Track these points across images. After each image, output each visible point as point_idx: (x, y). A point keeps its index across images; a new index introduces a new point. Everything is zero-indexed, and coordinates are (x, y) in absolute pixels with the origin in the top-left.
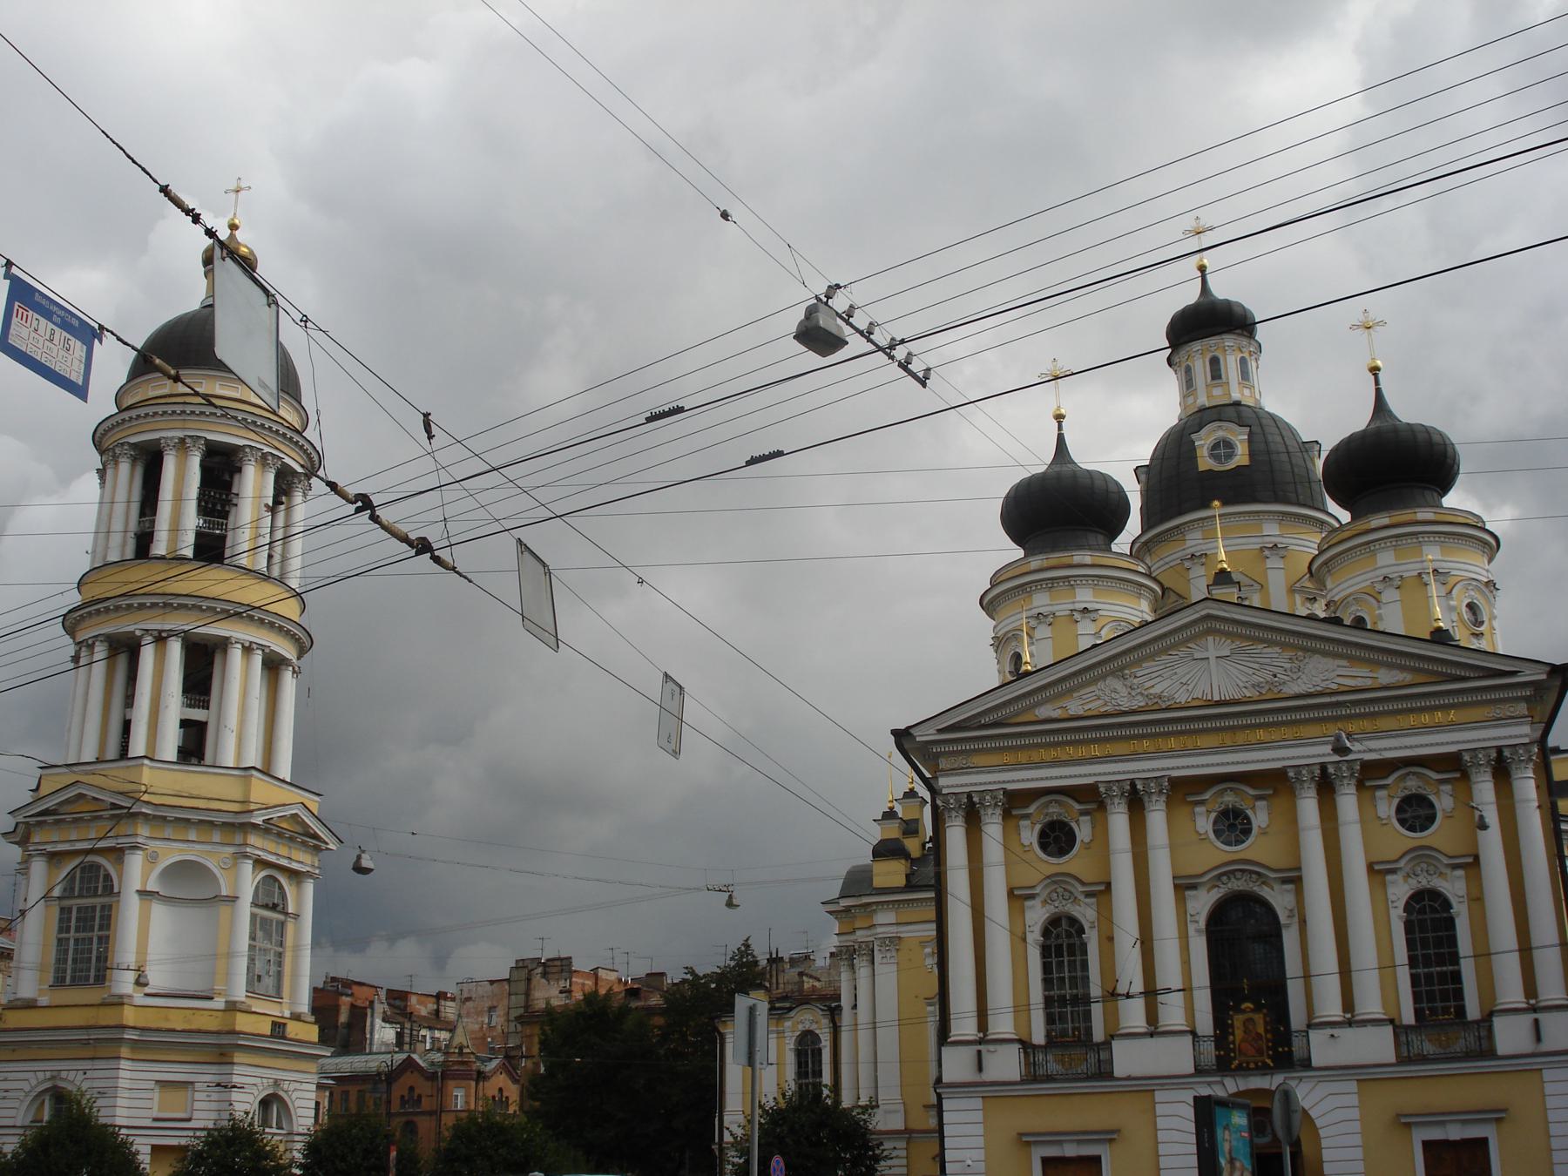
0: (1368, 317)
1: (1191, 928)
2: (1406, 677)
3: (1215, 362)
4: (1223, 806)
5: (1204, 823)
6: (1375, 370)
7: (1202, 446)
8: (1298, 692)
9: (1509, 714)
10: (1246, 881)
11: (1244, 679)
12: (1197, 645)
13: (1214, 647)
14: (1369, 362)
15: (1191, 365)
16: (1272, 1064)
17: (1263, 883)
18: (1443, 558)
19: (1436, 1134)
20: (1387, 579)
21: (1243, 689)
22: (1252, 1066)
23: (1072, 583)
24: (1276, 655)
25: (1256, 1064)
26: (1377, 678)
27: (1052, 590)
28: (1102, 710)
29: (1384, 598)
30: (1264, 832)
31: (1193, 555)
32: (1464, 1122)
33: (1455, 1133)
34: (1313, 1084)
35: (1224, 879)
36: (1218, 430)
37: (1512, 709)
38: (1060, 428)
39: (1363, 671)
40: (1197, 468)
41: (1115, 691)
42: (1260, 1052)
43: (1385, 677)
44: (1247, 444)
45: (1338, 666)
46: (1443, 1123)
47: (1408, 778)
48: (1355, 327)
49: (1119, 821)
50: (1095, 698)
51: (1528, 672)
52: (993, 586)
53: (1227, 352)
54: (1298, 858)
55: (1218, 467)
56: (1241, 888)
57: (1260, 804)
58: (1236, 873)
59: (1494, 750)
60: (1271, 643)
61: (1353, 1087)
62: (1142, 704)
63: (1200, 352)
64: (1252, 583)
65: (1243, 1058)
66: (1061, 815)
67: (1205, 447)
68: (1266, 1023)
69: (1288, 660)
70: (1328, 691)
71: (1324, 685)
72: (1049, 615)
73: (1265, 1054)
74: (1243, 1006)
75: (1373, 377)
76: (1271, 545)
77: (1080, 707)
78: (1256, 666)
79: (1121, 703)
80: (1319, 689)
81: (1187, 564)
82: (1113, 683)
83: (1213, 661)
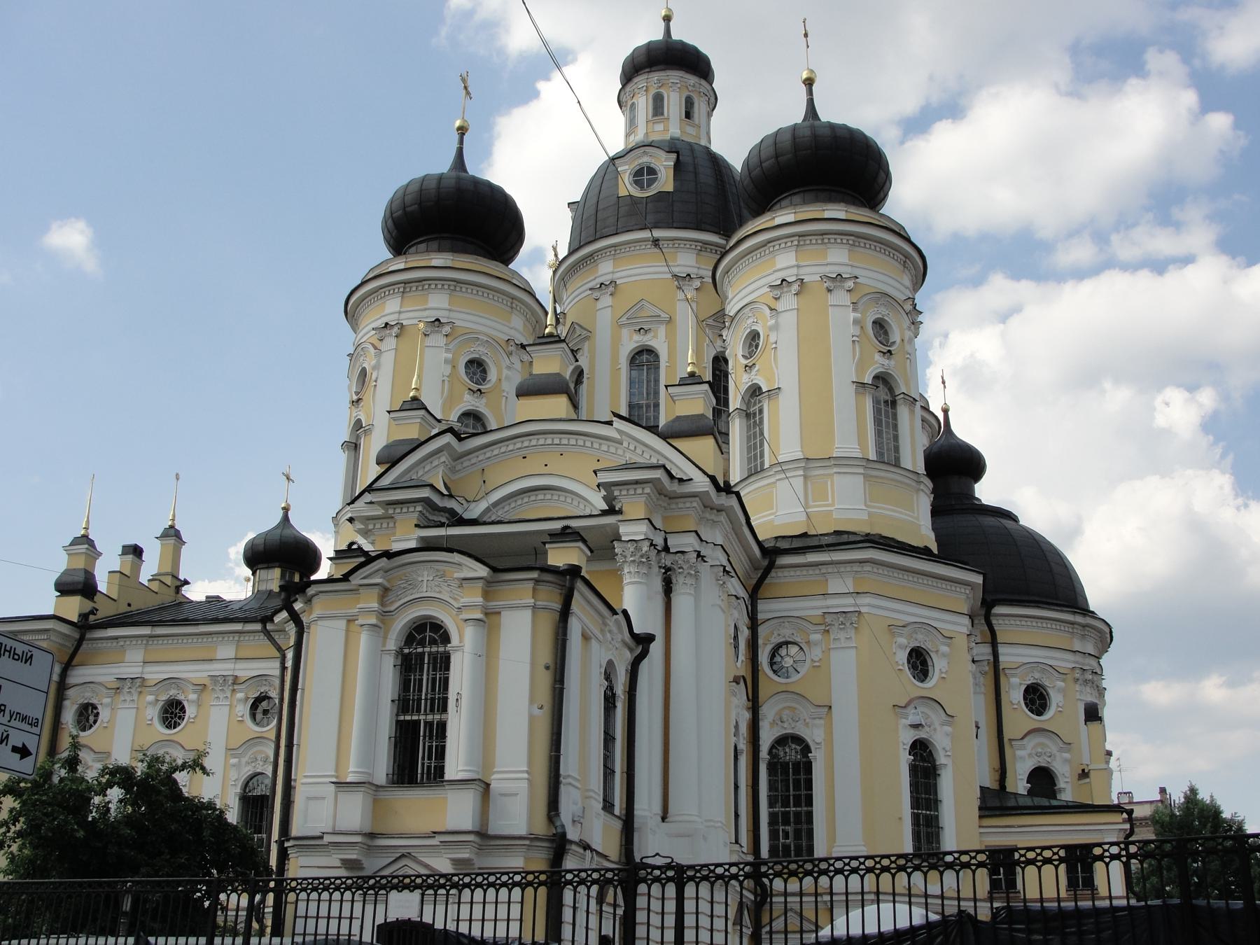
7: (625, 171)
55: (637, 193)
81: (597, 294)
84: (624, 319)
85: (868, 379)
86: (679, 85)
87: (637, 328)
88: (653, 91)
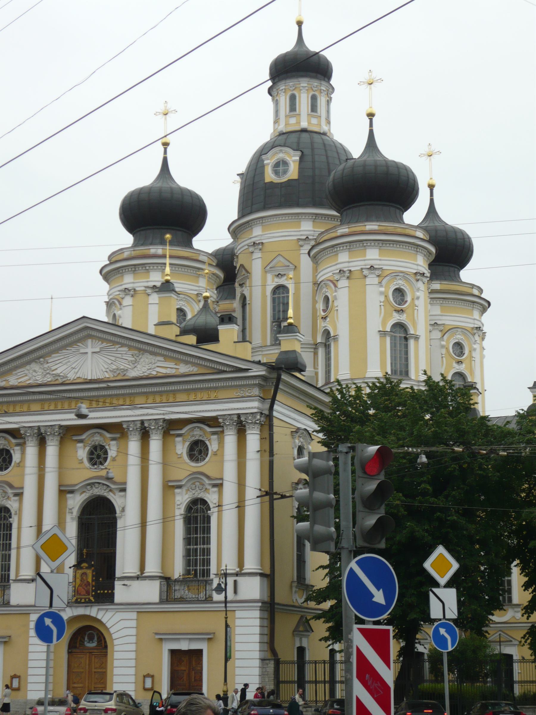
0: (371, 76)
1: (68, 517)
2: (195, 370)
3: (293, 98)
4: (93, 443)
5: (82, 452)
6: (371, 116)
7: (268, 164)
8: (134, 376)
9: (248, 394)
10: (101, 489)
11: (106, 367)
12: (82, 344)
13: (91, 347)
14: (367, 109)
15: (278, 99)
16: (93, 600)
17: (111, 491)
18: (380, 258)
19: (176, 646)
20: (342, 272)
21: (105, 373)
22: (83, 601)
23: (147, 268)
24: (125, 352)
25: (85, 599)
26: (178, 369)
27: (135, 272)
28: (28, 382)
29: (340, 284)
30: (114, 459)
31: (254, 243)
32: (190, 639)
33: (184, 646)
34: (114, 613)
35: (89, 487)
36: (279, 153)
37: (249, 391)
38: (165, 152)
39: (171, 365)
40: (264, 180)
41: (35, 371)
42: (88, 593)
43: (183, 369)
44: (297, 164)
45: (158, 361)
46: (179, 639)
47: (195, 429)
48: (362, 83)
49: (31, 451)
50: (25, 375)
51: (255, 370)
52: (111, 263)
53: (302, 92)
54: (126, 479)
56: (98, 493)
57: (113, 443)
58: (95, 484)
59: (236, 416)
60: (123, 345)
61: (134, 615)
62: (49, 380)
63: (284, 90)
64: (288, 264)
65: (79, 596)
66: (5, 445)
67: (270, 165)
68: (93, 576)
69: (131, 356)
70: (151, 376)
71: (148, 372)
72: (131, 290)
73: (91, 594)
74: (82, 565)
75: (369, 120)
76: (304, 237)
77: (16, 380)
78: (113, 358)
79: (38, 379)
80: (146, 374)
81: (251, 249)
82: (34, 366)
83: (90, 354)
84: (268, 268)
85: (388, 329)
86: (307, 88)
87: (277, 273)
88: (289, 93)
